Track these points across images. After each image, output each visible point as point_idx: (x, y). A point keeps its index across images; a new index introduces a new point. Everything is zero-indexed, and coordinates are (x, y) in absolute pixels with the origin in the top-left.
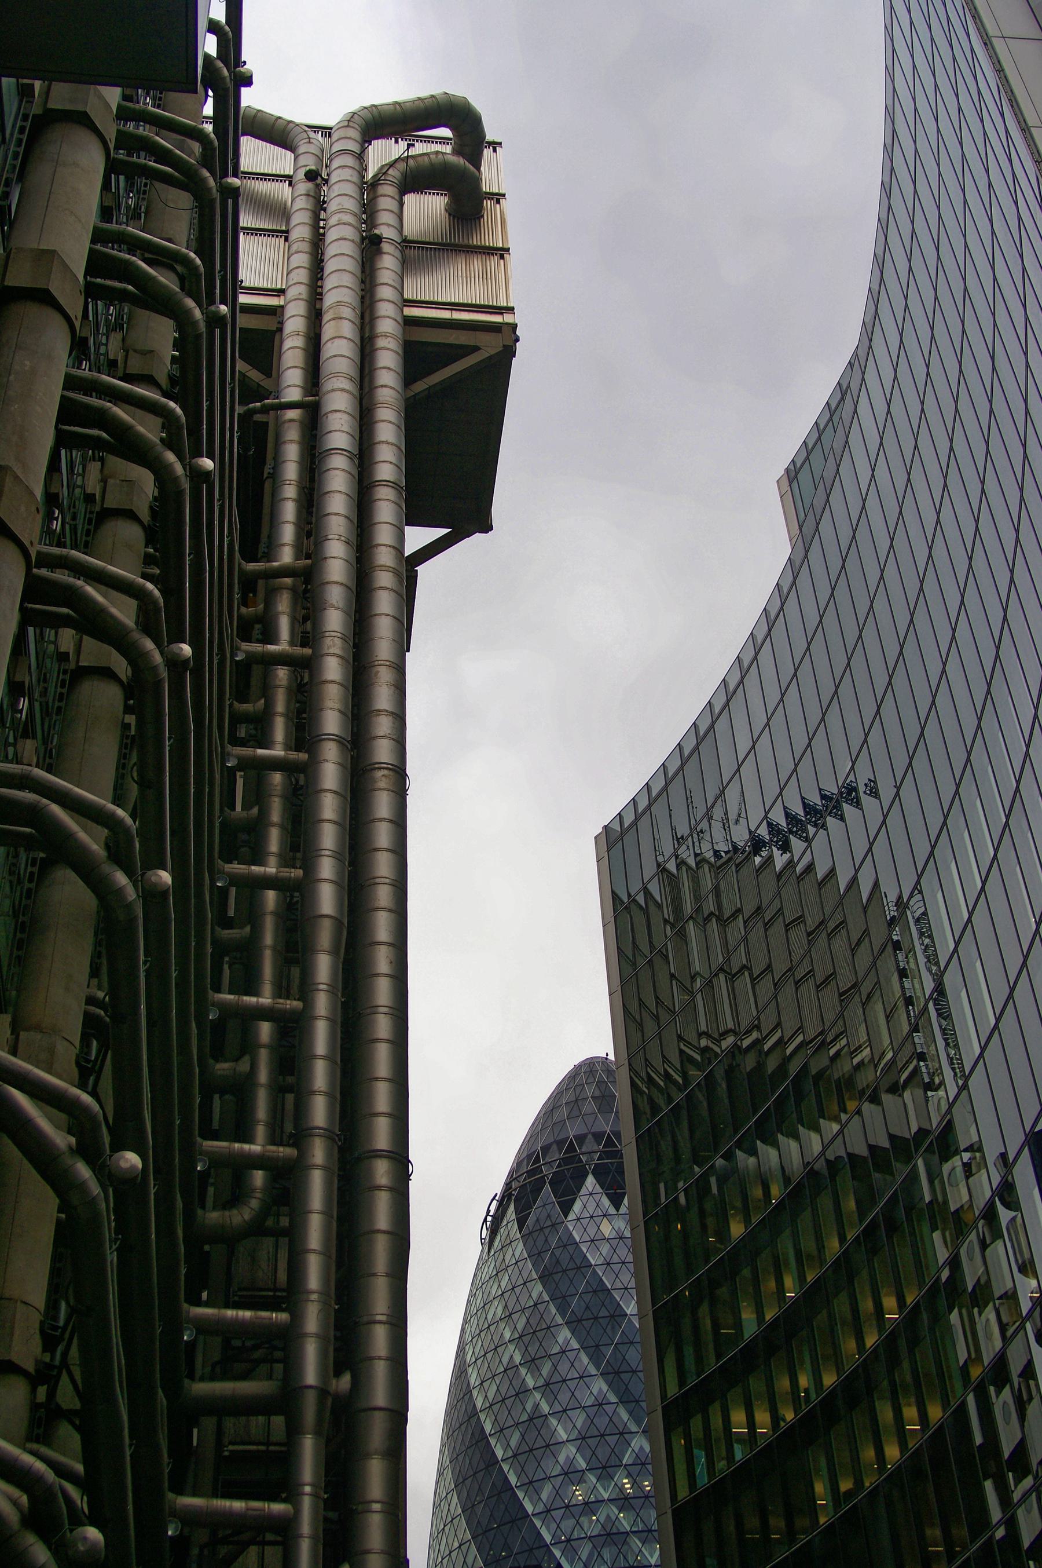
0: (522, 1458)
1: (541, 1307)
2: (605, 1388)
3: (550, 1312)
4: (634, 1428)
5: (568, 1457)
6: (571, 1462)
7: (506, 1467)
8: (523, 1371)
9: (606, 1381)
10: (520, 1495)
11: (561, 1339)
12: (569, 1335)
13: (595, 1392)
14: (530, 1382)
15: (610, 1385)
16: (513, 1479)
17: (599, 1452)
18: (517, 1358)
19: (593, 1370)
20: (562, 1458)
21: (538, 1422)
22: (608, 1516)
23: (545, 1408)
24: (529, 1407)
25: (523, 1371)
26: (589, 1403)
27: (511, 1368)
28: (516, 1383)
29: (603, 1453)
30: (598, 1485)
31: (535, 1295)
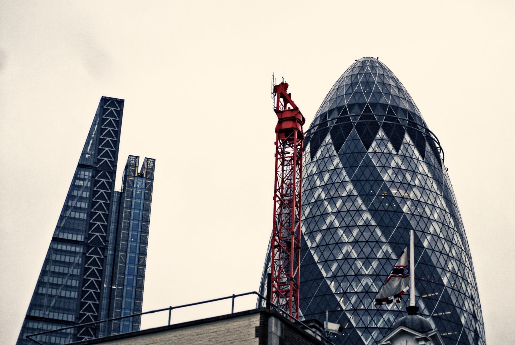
0: (322, 248)
1: (338, 171)
2: (370, 218)
3: (342, 174)
4: (383, 239)
5: (347, 251)
6: (348, 253)
7: (312, 252)
8: (326, 203)
9: (371, 214)
10: (320, 267)
11: (348, 189)
12: (352, 188)
13: (365, 218)
14: (329, 209)
15: (373, 216)
16: (316, 258)
17: (365, 250)
18: (323, 196)
19: (364, 208)
20: (344, 251)
21: (333, 231)
22: (367, 283)
23: (337, 224)
24: (328, 222)
25: (326, 203)
26: (361, 224)
27: (319, 200)
28: (322, 210)
29: (367, 250)
30: (363, 267)
31: (335, 163)
